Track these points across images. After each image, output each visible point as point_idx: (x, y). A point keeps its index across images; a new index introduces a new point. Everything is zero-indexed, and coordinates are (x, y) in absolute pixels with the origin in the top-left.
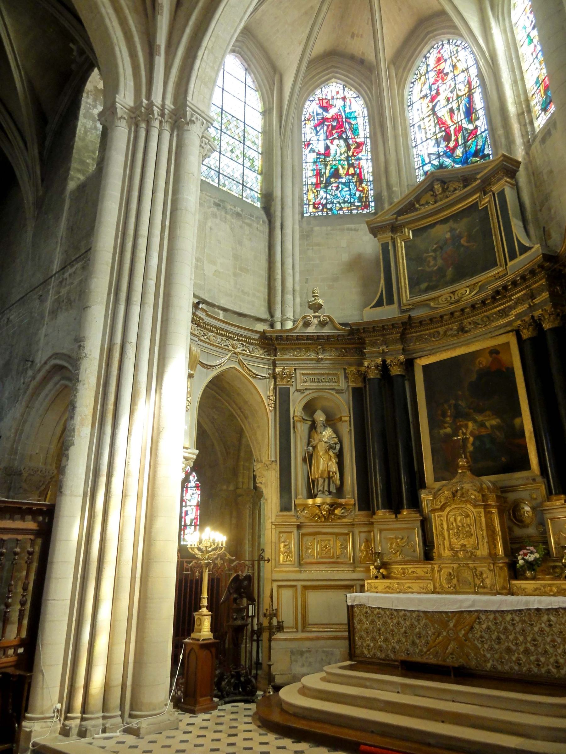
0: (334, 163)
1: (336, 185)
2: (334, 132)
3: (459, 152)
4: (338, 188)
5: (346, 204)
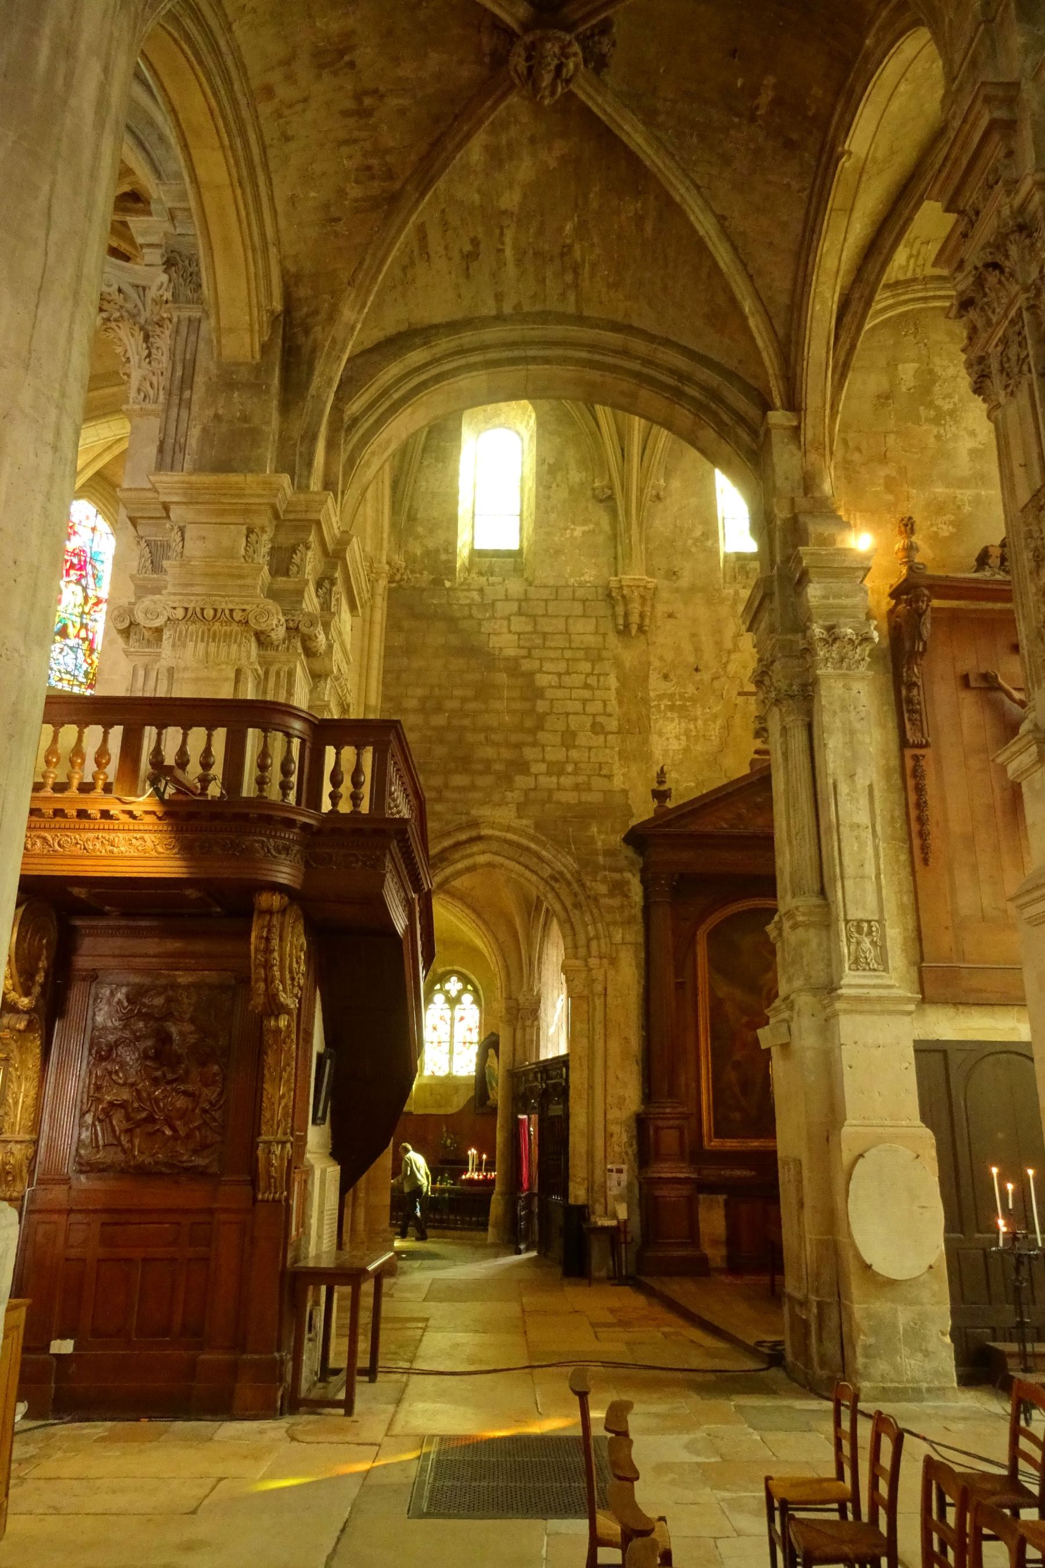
0: (64, 615)
1: (62, 646)
2: (72, 572)
4: (62, 650)
5: (68, 677)
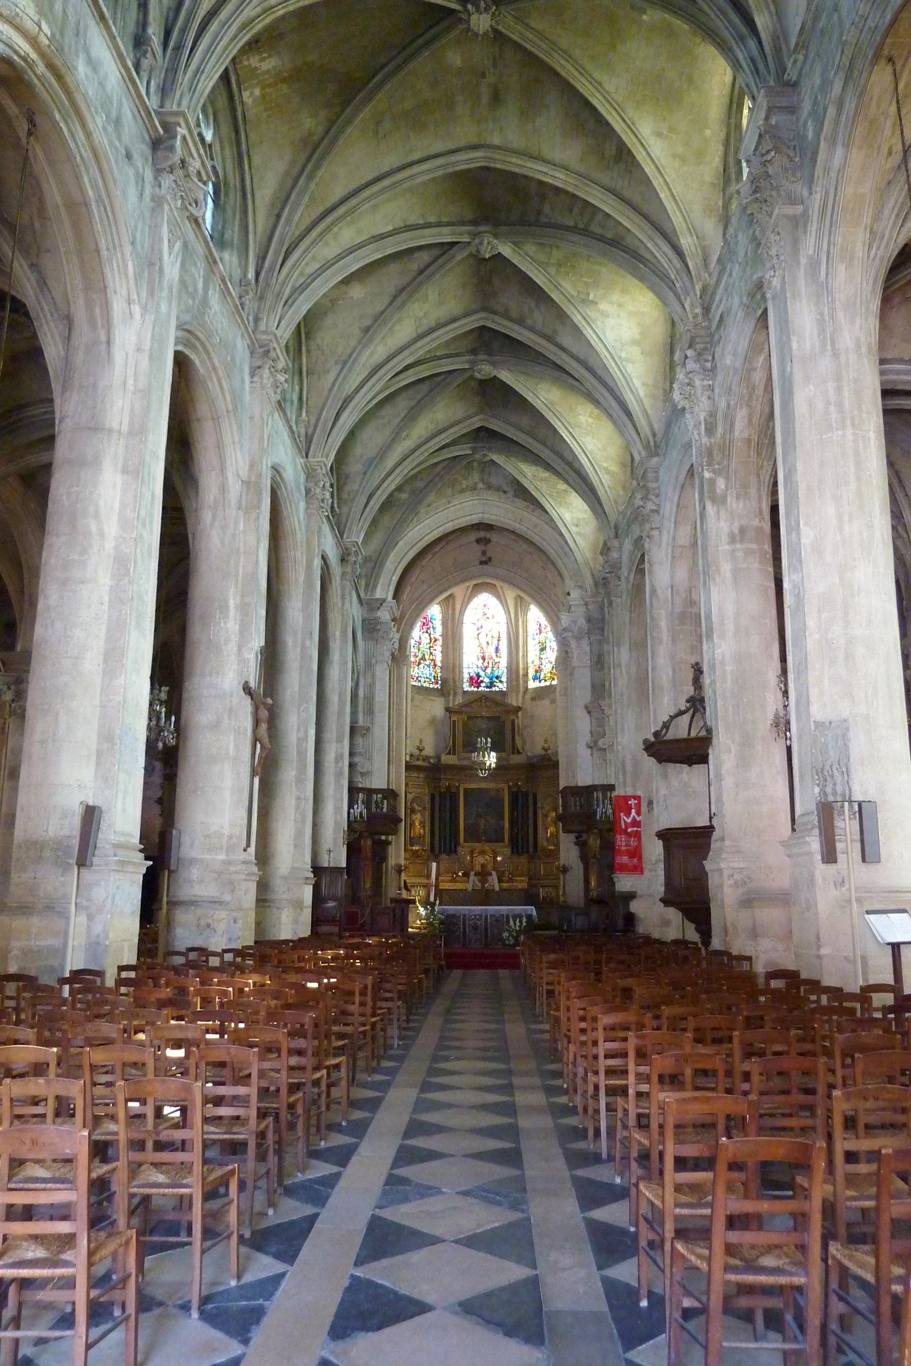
3: (489, 671)
